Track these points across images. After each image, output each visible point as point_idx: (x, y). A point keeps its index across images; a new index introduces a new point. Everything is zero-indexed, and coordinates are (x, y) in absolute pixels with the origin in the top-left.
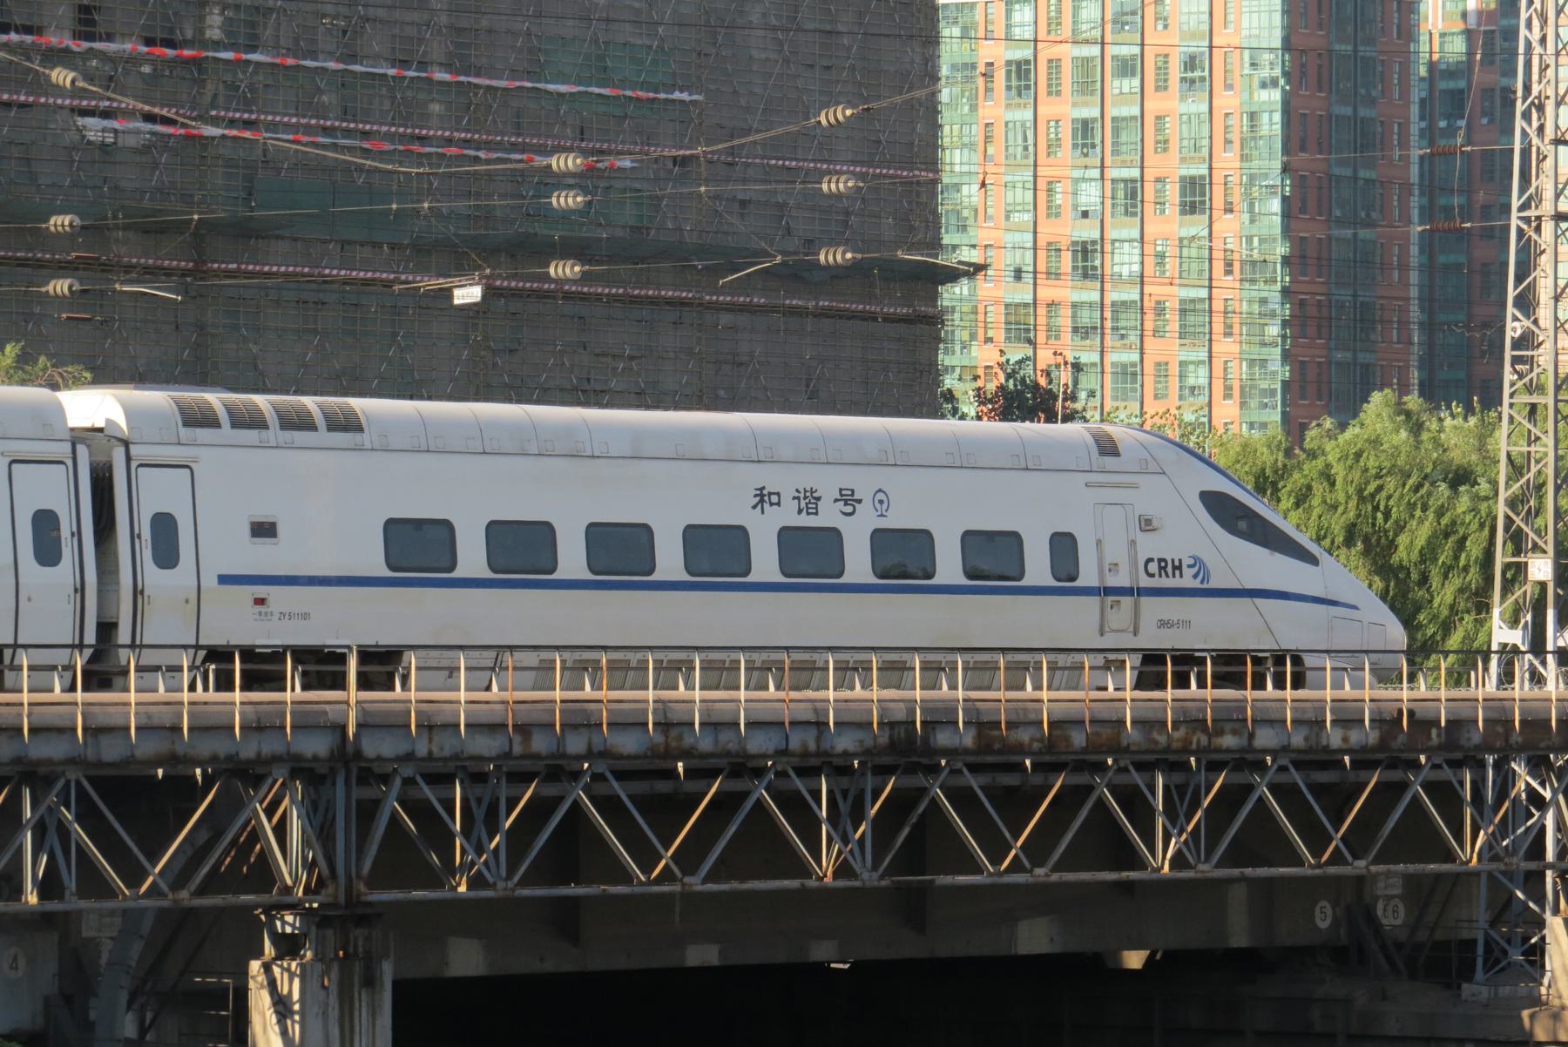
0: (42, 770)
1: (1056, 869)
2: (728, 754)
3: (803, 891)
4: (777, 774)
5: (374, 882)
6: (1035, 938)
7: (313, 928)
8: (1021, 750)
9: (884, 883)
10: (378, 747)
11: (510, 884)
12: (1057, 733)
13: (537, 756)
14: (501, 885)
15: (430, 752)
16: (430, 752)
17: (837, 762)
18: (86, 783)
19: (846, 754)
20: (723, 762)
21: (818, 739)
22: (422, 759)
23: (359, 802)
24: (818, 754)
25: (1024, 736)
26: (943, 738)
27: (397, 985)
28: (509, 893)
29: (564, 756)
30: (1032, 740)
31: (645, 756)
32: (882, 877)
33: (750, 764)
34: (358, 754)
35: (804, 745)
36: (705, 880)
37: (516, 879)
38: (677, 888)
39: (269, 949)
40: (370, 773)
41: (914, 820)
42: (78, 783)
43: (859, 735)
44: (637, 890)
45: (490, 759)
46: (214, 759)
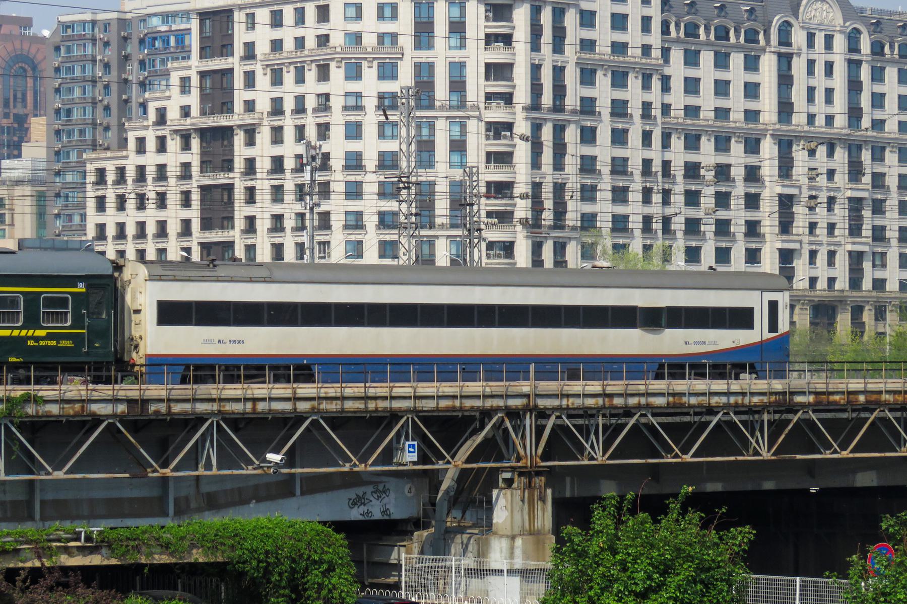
0: (400, 414)
1: (851, 452)
2: (700, 406)
3: (736, 461)
4: (724, 414)
5: (544, 458)
6: (866, 480)
7: (516, 476)
8: (835, 403)
9: (773, 458)
10: (542, 403)
11: (604, 458)
12: (851, 396)
13: (616, 407)
14: (600, 459)
15: (568, 405)
16: (568, 405)
17: (754, 409)
18: (416, 419)
19: (755, 406)
20: (704, 410)
21: (743, 400)
22: (565, 409)
23: (537, 426)
24: (743, 405)
25: (837, 398)
26: (799, 399)
27: (555, 502)
28: (603, 462)
29: (626, 406)
30: (841, 399)
31: (664, 407)
32: (773, 455)
33: (715, 410)
34: (536, 407)
35: (736, 403)
36: (693, 456)
37: (607, 456)
38: (679, 460)
39: (501, 484)
40: (543, 414)
41: (786, 431)
42: (413, 420)
43: (761, 398)
44: (661, 461)
45: (594, 408)
46: (472, 409)
